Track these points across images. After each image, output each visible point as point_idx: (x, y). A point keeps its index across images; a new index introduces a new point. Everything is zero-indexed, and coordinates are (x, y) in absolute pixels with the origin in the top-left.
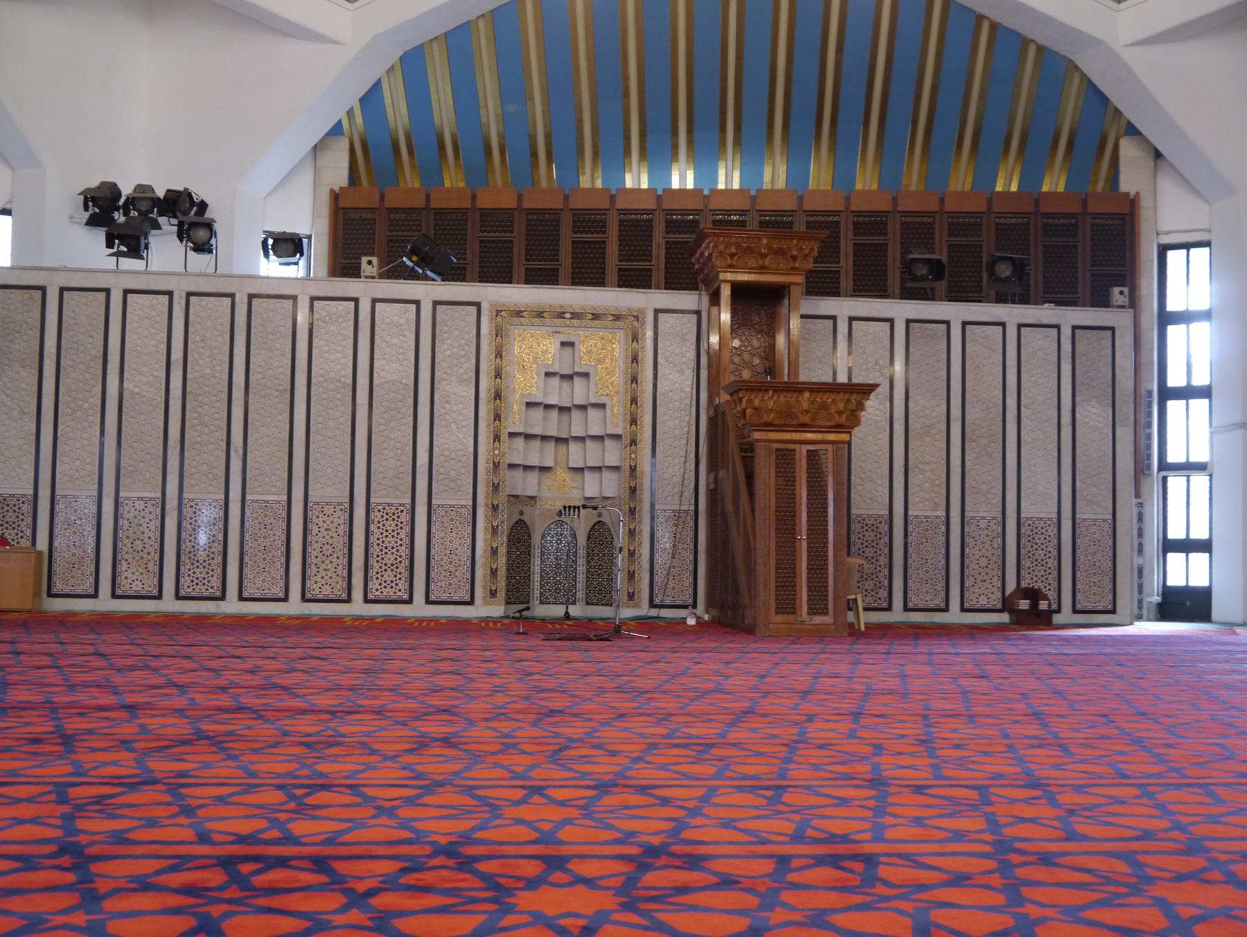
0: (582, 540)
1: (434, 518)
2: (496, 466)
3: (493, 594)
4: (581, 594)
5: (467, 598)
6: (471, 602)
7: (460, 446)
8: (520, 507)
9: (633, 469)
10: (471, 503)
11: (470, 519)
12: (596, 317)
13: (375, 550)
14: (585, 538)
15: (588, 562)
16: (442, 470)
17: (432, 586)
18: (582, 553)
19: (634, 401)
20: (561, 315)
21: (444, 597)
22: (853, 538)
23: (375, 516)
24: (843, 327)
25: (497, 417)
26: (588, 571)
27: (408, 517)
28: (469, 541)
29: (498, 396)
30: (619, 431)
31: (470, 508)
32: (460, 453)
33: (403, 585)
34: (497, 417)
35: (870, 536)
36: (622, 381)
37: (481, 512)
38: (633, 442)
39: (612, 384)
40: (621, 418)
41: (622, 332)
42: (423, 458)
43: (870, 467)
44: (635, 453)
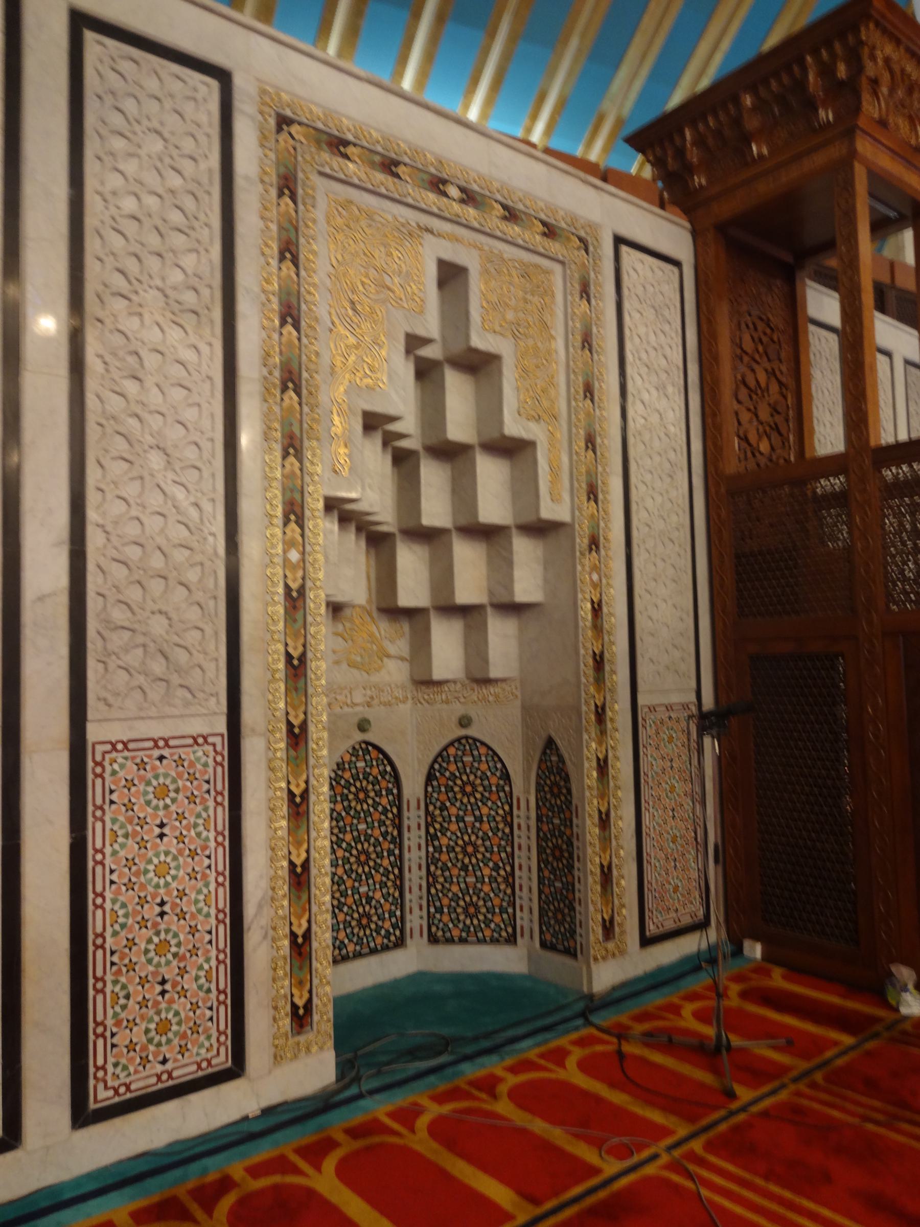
0: (413, 786)
1: (95, 793)
2: (295, 600)
3: (301, 1017)
4: (415, 920)
5: (223, 1060)
10: (221, 726)
11: (222, 783)
12: (511, 215)
14: (421, 779)
15: (431, 838)
16: (119, 615)
17: (98, 1052)
18: (413, 817)
20: (438, 184)
21: (144, 1081)
25: (292, 446)
26: (431, 861)
28: (222, 859)
29: (291, 379)
31: (222, 745)
34: (292, 446)
37: (254, 751)
38: (594, 543)
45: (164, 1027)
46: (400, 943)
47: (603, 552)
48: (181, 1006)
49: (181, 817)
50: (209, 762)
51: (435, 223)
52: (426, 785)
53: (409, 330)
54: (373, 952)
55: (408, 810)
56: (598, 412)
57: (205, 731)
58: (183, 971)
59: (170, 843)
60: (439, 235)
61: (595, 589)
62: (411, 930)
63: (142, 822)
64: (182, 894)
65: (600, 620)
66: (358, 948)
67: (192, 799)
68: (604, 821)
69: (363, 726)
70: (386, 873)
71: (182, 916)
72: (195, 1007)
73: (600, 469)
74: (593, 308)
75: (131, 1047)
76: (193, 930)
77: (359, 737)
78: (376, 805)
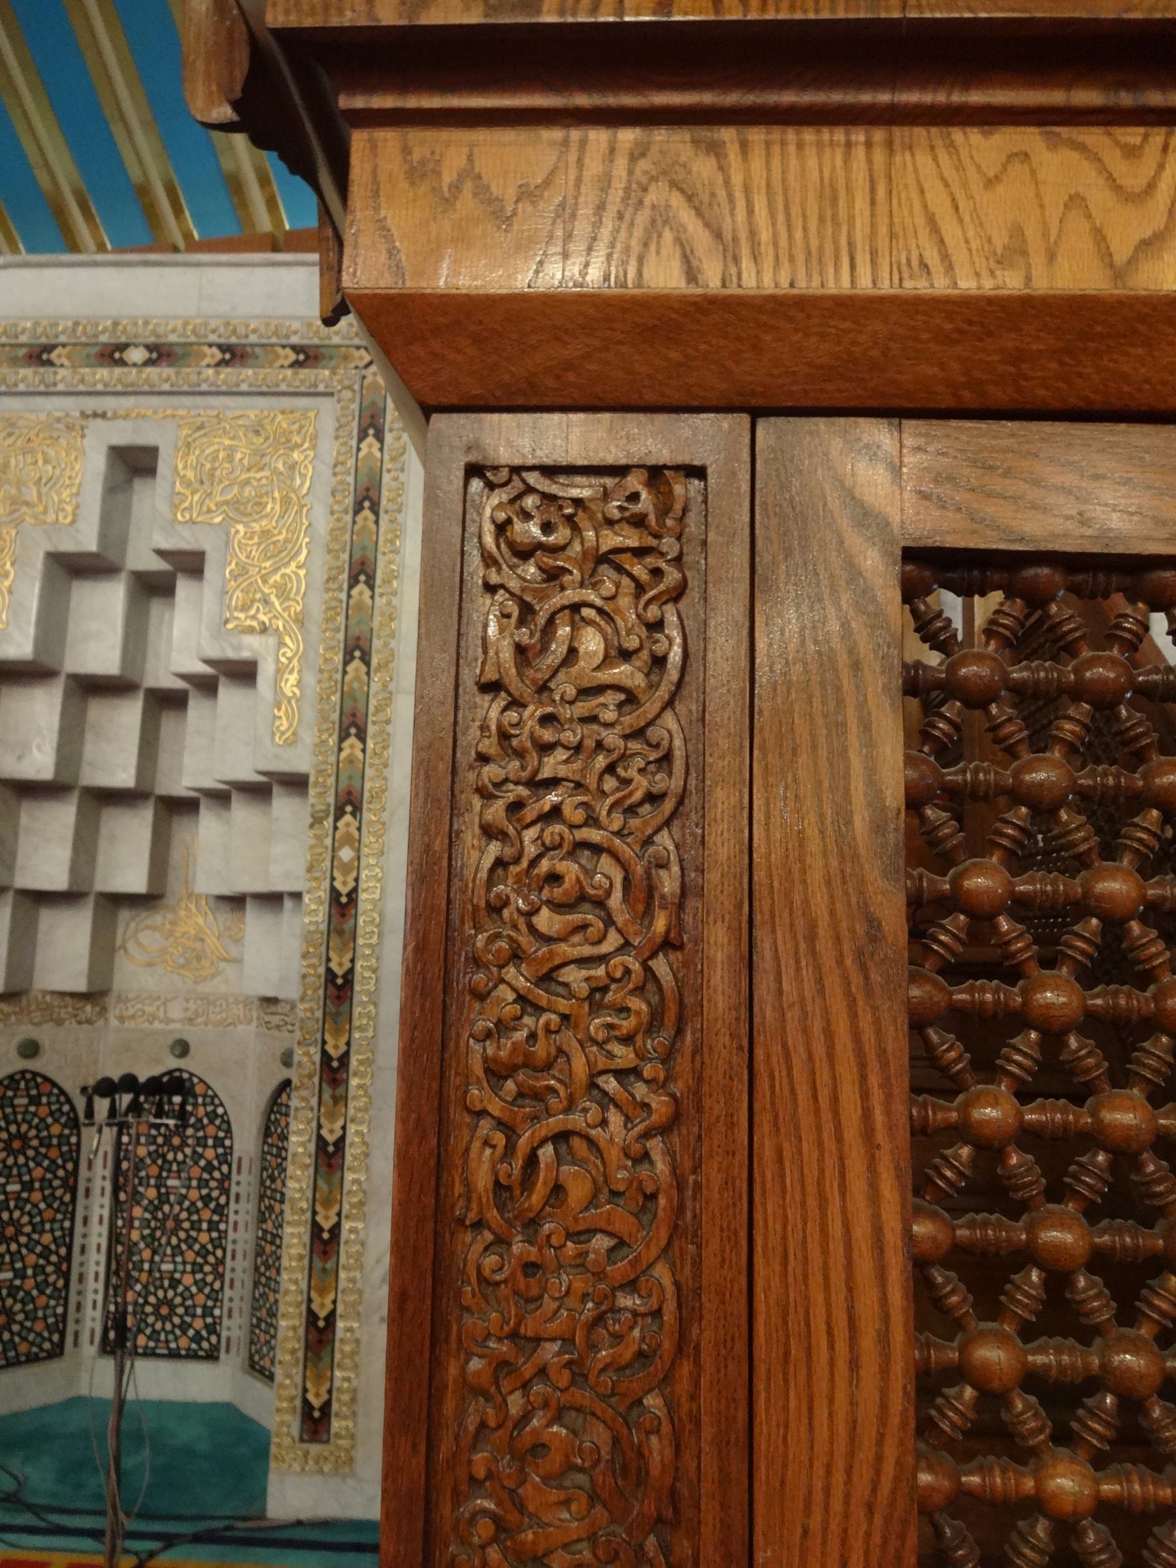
8: (26, 1031)
9: (343, 906)
12: (234, 354)
19: (357, 648)
20: (112, 355)
30: (300, 761)
36: (320, 575)
38: (349, 802)
39: (283, 592)
40: (310, 714)
41: (326, 404)
44: (357, 845)
46: (212, 1356)
47: (367, 816)
51: (108, 404)
52: (265, 1142)
53: (51, 549)
54: (174, 1355)
55: (239, 1172)
56: (380, 602)
60: (116, 416)
61: (346, 873)
62: (228, 1339)
65: (352, 921)
66: (152, 1344)
68: (325, 1243)
69: (182, 1048)
70: (204, 1253)
73: (375, 686)
74: (386, 448)
77: (172, 1063)
78: (197, 1156)
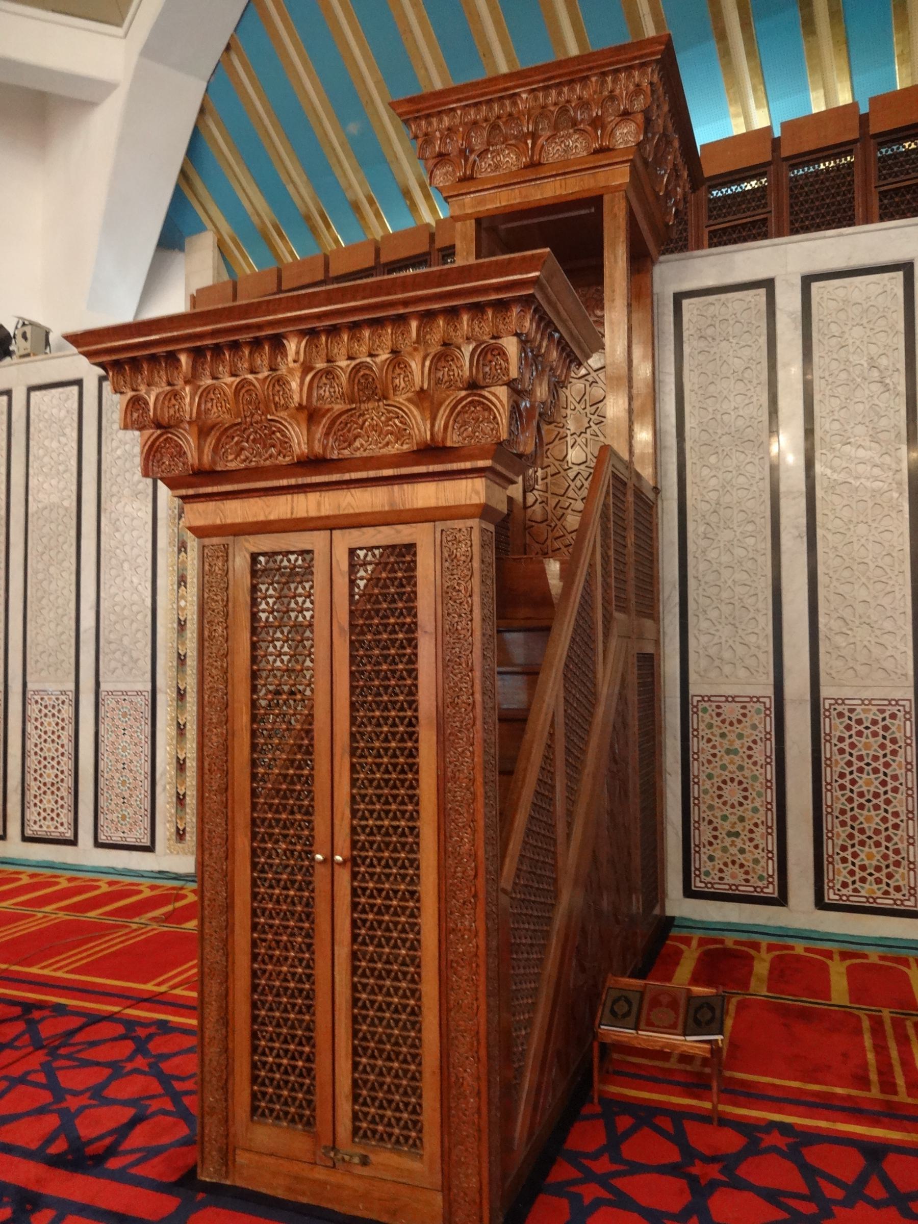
1: (102, 713)
3: (180, 835)
6: (150, 849)
7: (135, 597)
11: (148, 714)
13: (32, 762)
16: (112, 637)
21: (116, 838)
22: (827, 750)
23: (33, 710)
24: (788, 301)
27: (71, 710)
28: (147, 749)
31: (149, 696)
32: (135, 608)
33: (66, 816)
35: (869, 746)
37: (160, 698)
42: (87, 621)
43: (863, 594)
45: (124, 818)
48: (130, 810)
49: (131, 727)
50: (143, 703)
57: (141, 689)
58: (131, 796)
59: (127, 738)
63: (117, 727)
64: (131, 762)
67: (135, 719)
71: (131, 771)
72: (135, 813)
75: (112, 821)
76: (135, 779)
